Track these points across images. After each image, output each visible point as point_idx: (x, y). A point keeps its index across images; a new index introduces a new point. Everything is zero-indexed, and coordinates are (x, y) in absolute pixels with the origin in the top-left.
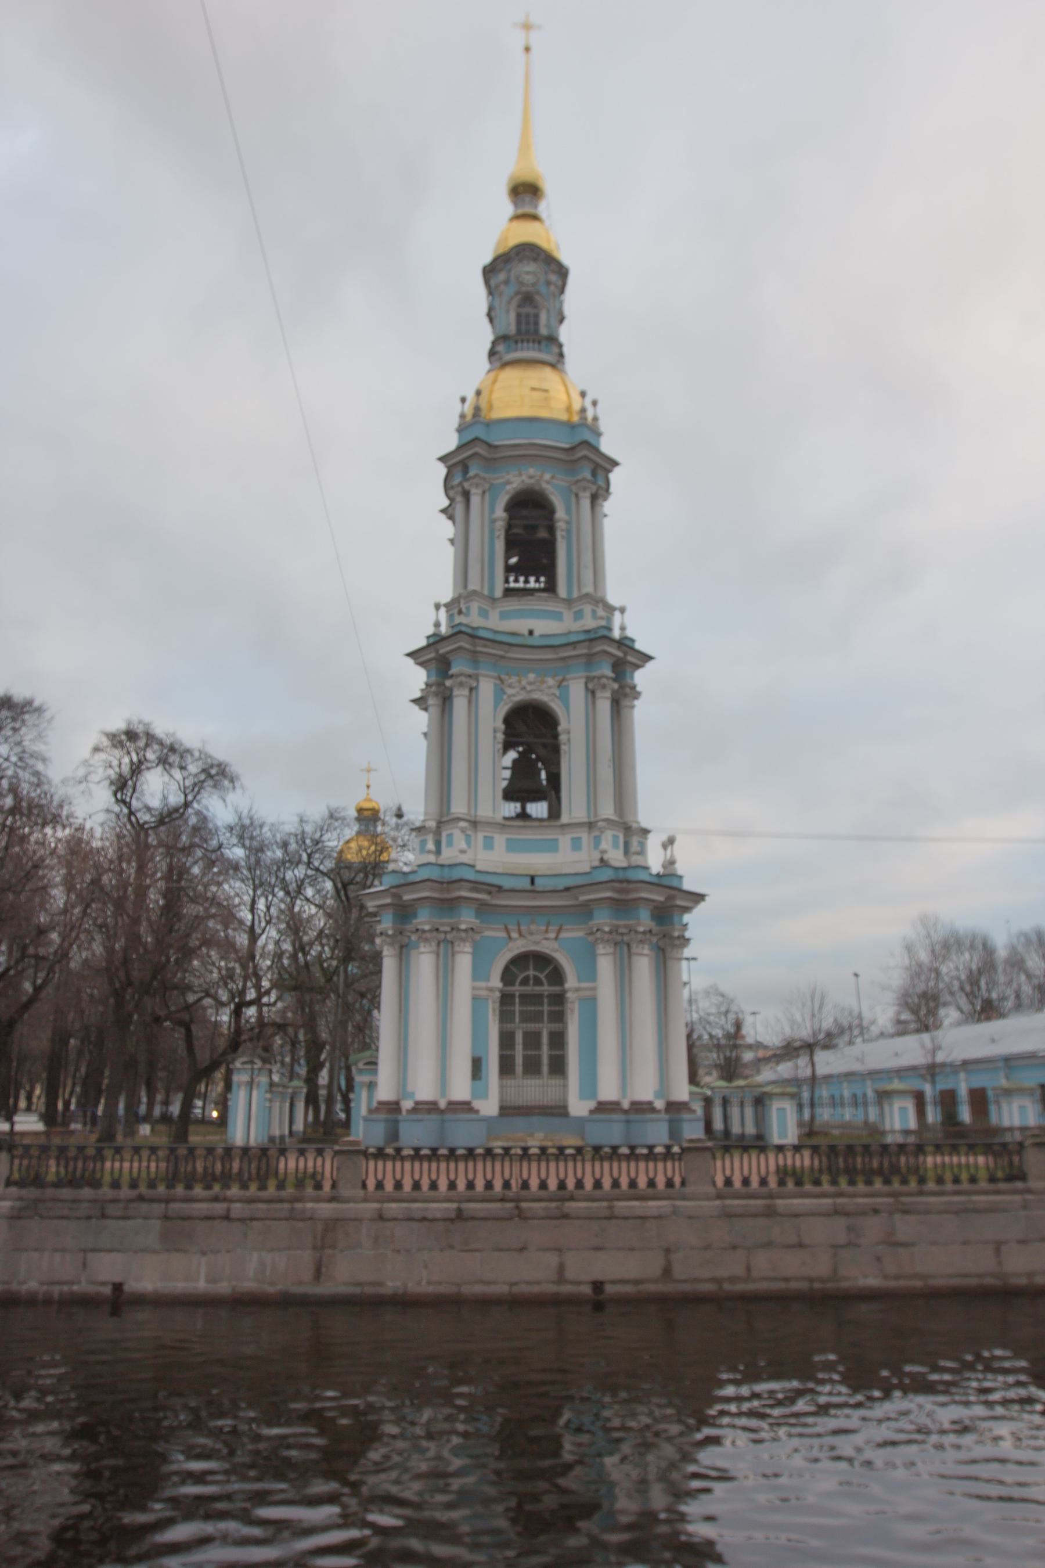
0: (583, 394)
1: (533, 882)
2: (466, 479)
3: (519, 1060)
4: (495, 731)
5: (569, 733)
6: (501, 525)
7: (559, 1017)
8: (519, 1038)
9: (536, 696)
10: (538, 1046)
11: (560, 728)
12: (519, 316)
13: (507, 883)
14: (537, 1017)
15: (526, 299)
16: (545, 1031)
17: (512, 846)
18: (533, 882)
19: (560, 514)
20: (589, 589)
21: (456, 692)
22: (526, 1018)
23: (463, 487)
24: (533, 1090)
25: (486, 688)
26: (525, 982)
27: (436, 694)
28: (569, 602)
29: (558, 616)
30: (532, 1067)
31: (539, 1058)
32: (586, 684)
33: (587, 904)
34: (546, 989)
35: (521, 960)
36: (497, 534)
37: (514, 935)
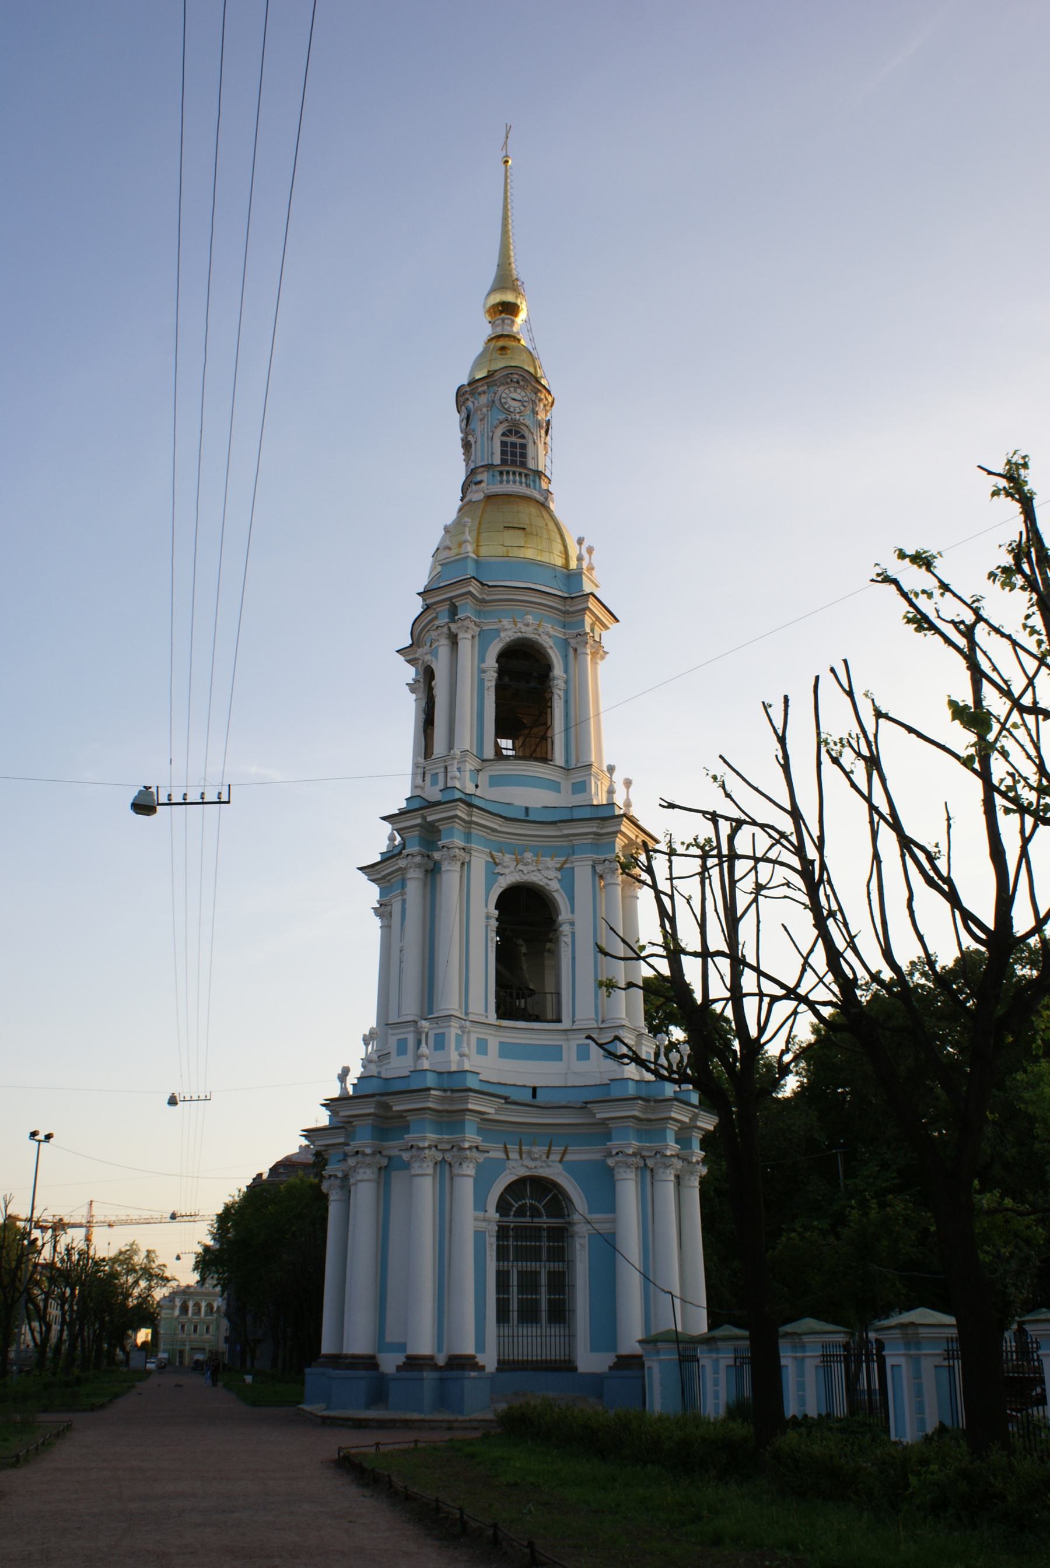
0: (580, 541)
1: (534, 1096)
2: (453, 621)
3: (514, 1305)
4: (488, 917)
5: (572, 924)
8: (514, 1280)
9: (536, 878)
10: (535, 1288)
11: (561, 918)
12: (504, 444)
13: (515, 1096)
14: (534, 1255)
16: (544, 1269)
17: (507, 1051)
18: (534, 1096)
19: (558, 671)
21: (445, 867)
22: (522, 1254)
23: (449, 628)
24: (536, 1341)
25: (479, 864)
26: (520, 1212)
27: (419, 866)
29: (555, 787)
30: (529, 1315)
31: (537, 1302)
32: (593, 867)
33: (604, 1122)
34: (545, 1221)
35: (516, 1188)
36: (487, 684)
37: (514, 1156)
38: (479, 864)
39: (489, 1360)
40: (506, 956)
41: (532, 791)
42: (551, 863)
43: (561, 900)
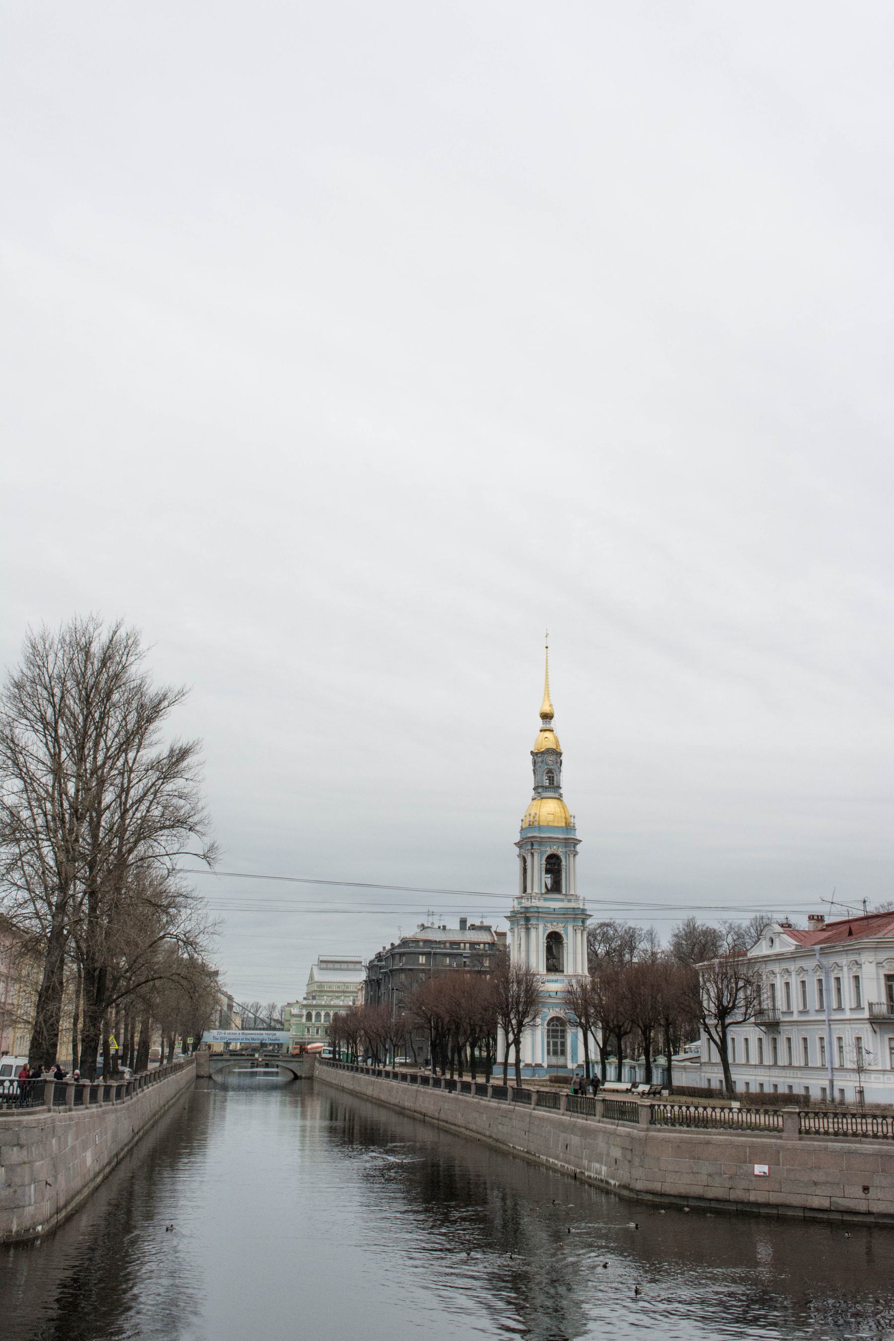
6: (544, 866)
7: (563, 1037)
9: (557, 930)
15: (547, 768)
16: (559, 1041)
19: (563, 863)
20: (572, 892)
22: (553, 1037)
25: (541, 927)
26: (553, 1025)
28: (566, 895)
29: (562, 900)
30: (555, 1053)
34: (559, 1028)
35: (552, 1019)
38: (541, 927)
39: (545, 1065)
40: (549, 949)
41: (555, 904)
42: (560, 925)
43: (564, 936)
